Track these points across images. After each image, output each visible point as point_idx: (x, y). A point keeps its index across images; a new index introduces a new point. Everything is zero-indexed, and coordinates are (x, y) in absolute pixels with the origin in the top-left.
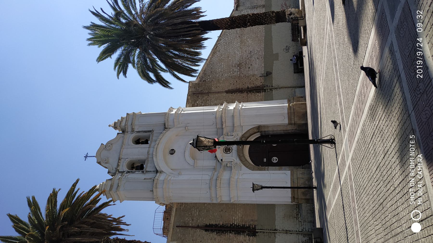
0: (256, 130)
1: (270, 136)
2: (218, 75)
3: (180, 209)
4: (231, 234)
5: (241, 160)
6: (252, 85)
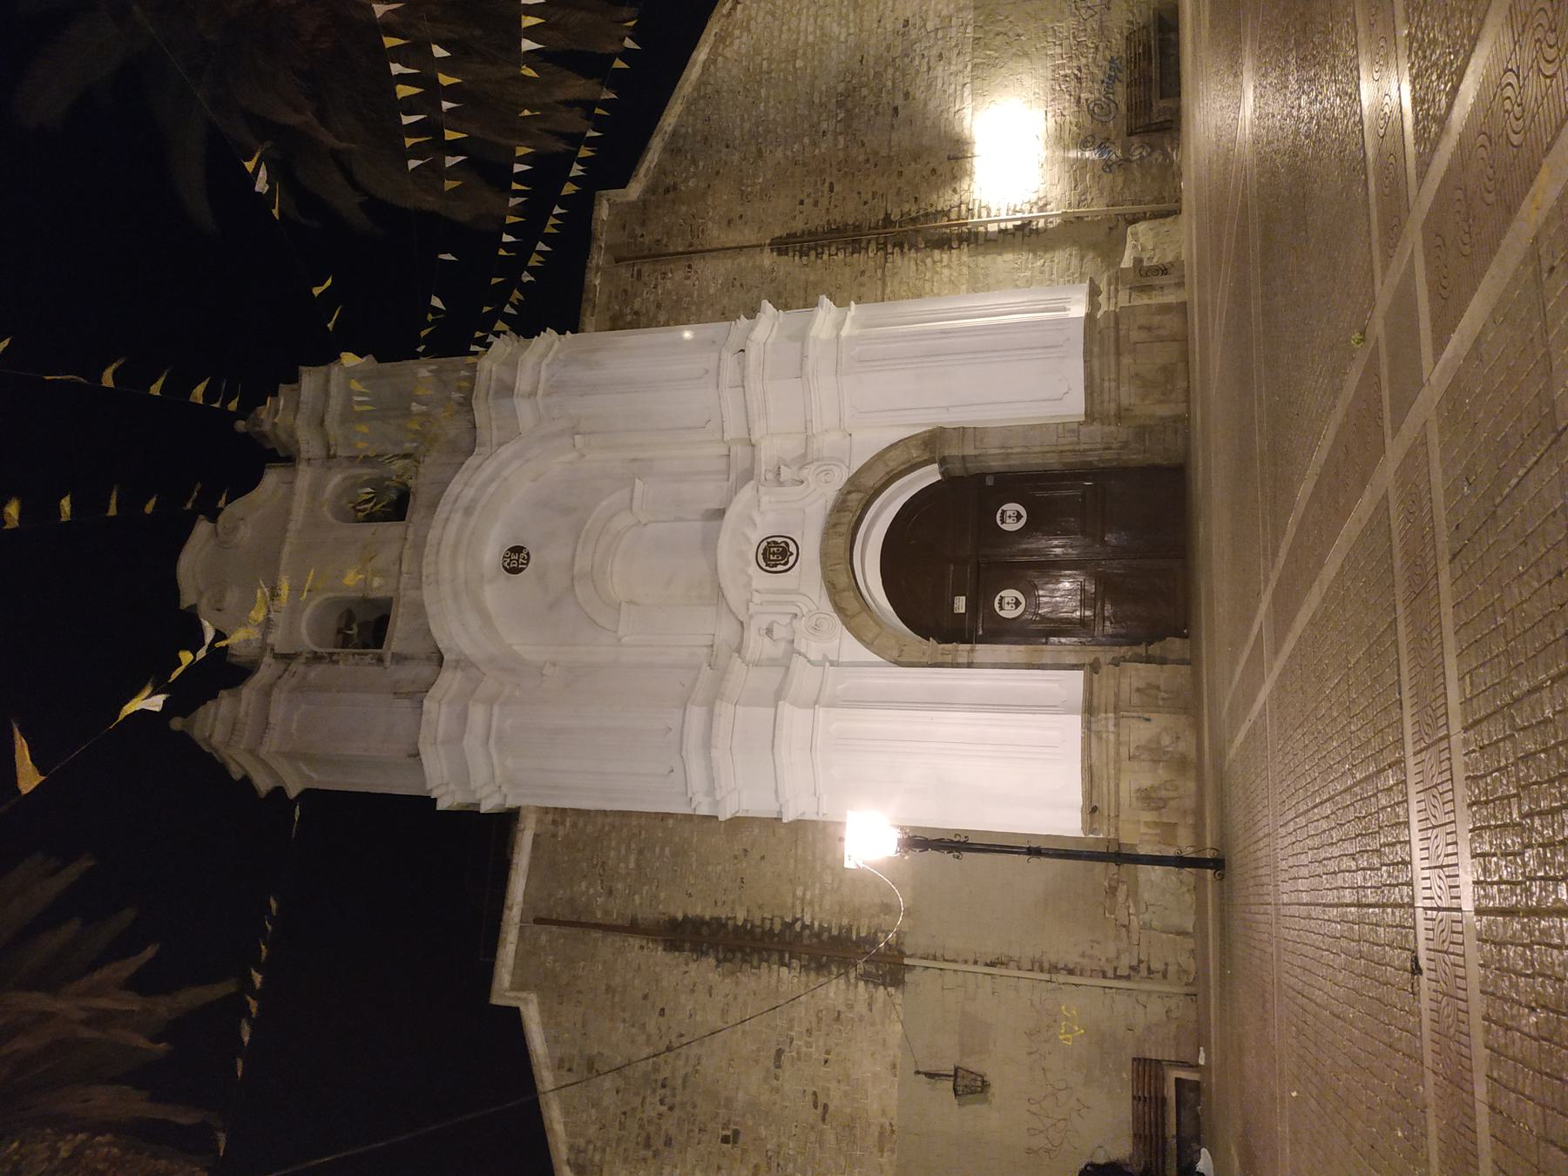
1: (990, 482)
2: (736, 157)
3: (554, 836)
4: (784, 970)
5: (839, 609)
6: (906, 208)
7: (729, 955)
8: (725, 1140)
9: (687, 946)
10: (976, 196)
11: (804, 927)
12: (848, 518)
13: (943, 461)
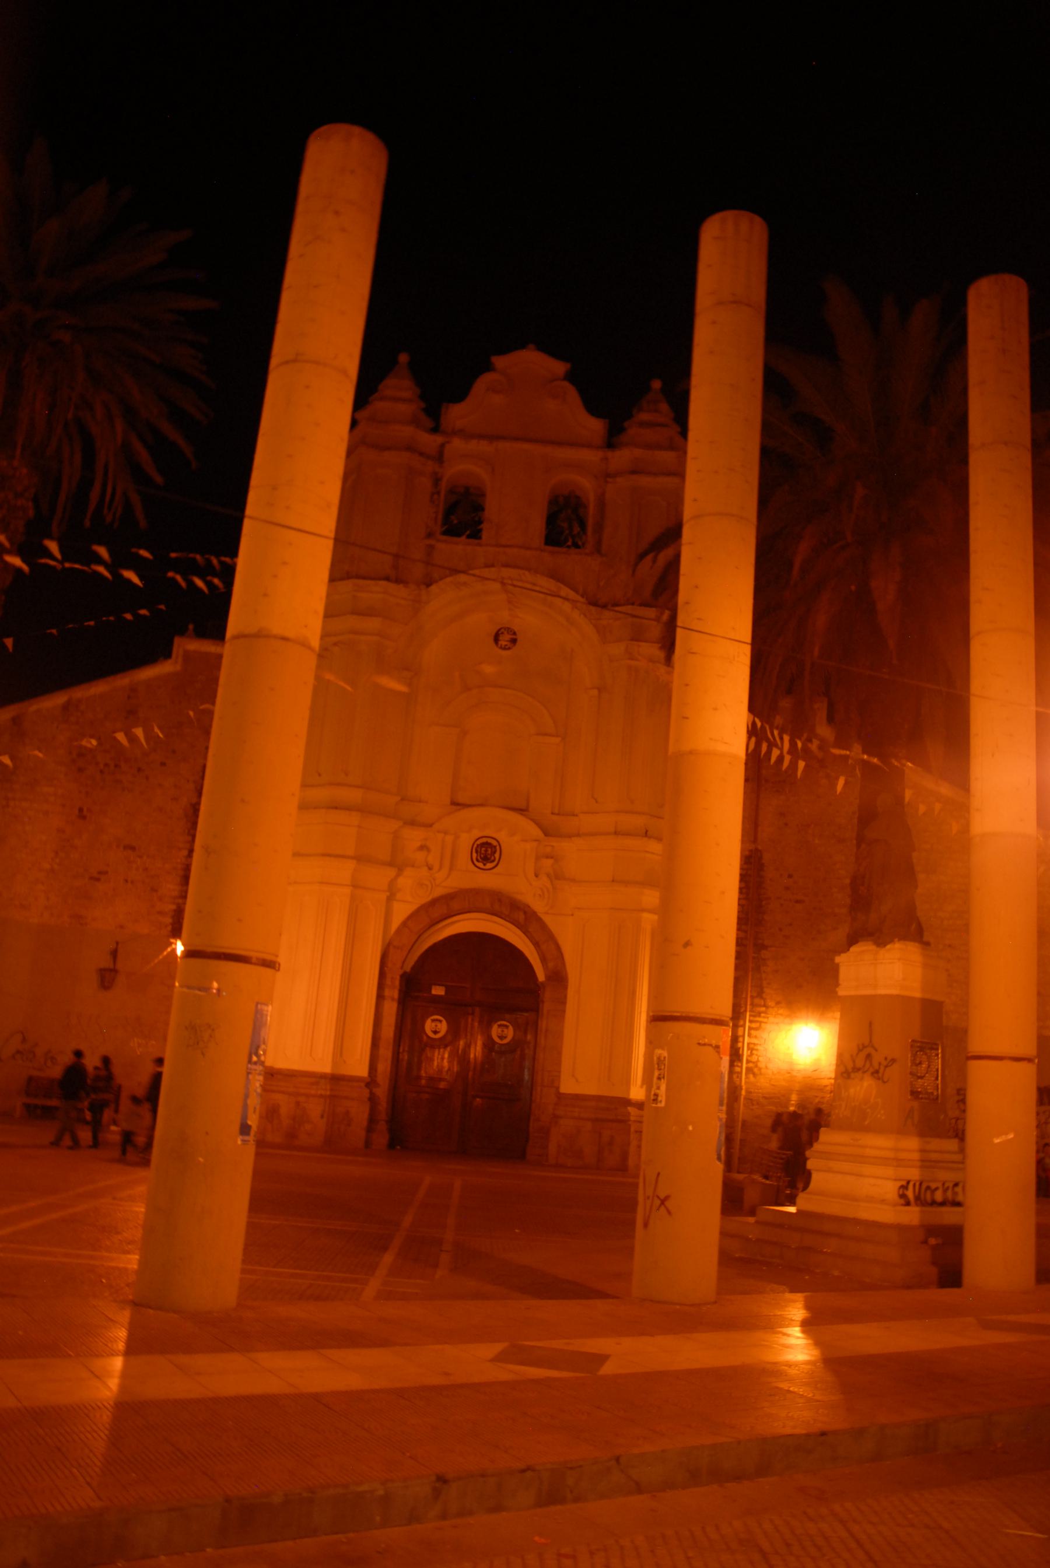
0: (551, 965)
5: (434, 902)
8: (81, 810)
10: (771, 1019)
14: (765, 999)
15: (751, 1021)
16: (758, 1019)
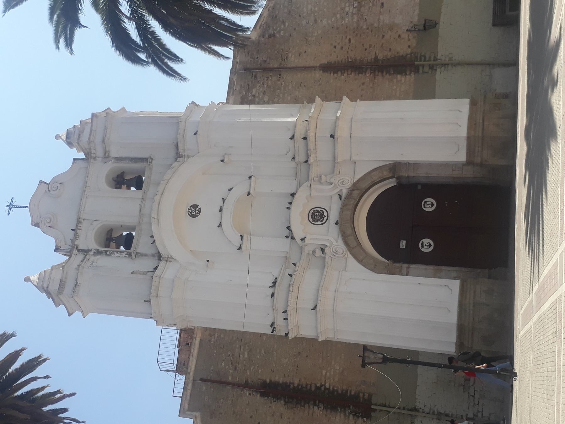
0: (386, 174)
1: (419, 187)
2: (304, 23)
4: (316, 408)
7: (291, 400)
9: (271, 395)
11: (326, 388)
12: (352, 202)
13: (398, 178)
14: (407, 55)
15: (421, 61)
16: (419, 58)
